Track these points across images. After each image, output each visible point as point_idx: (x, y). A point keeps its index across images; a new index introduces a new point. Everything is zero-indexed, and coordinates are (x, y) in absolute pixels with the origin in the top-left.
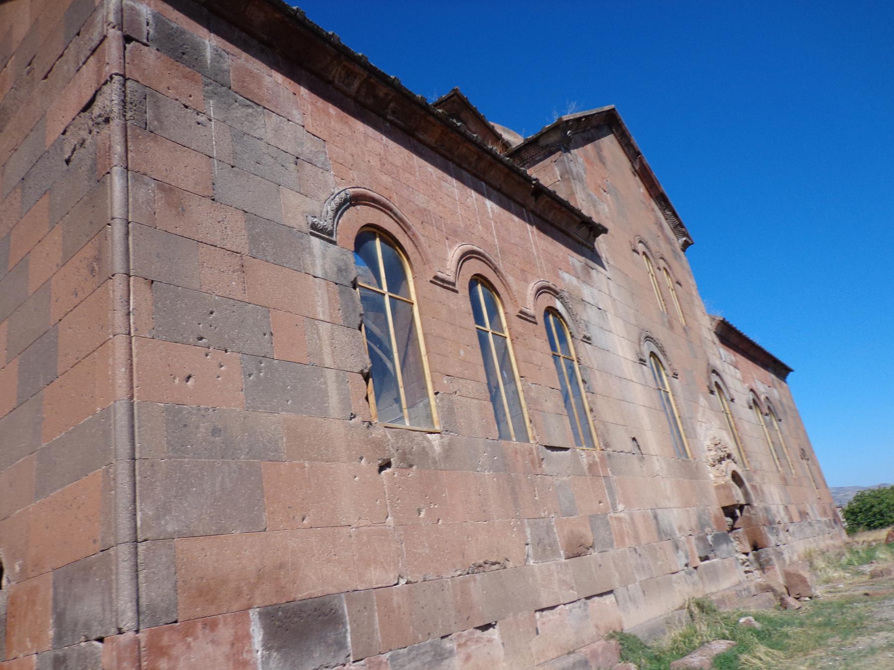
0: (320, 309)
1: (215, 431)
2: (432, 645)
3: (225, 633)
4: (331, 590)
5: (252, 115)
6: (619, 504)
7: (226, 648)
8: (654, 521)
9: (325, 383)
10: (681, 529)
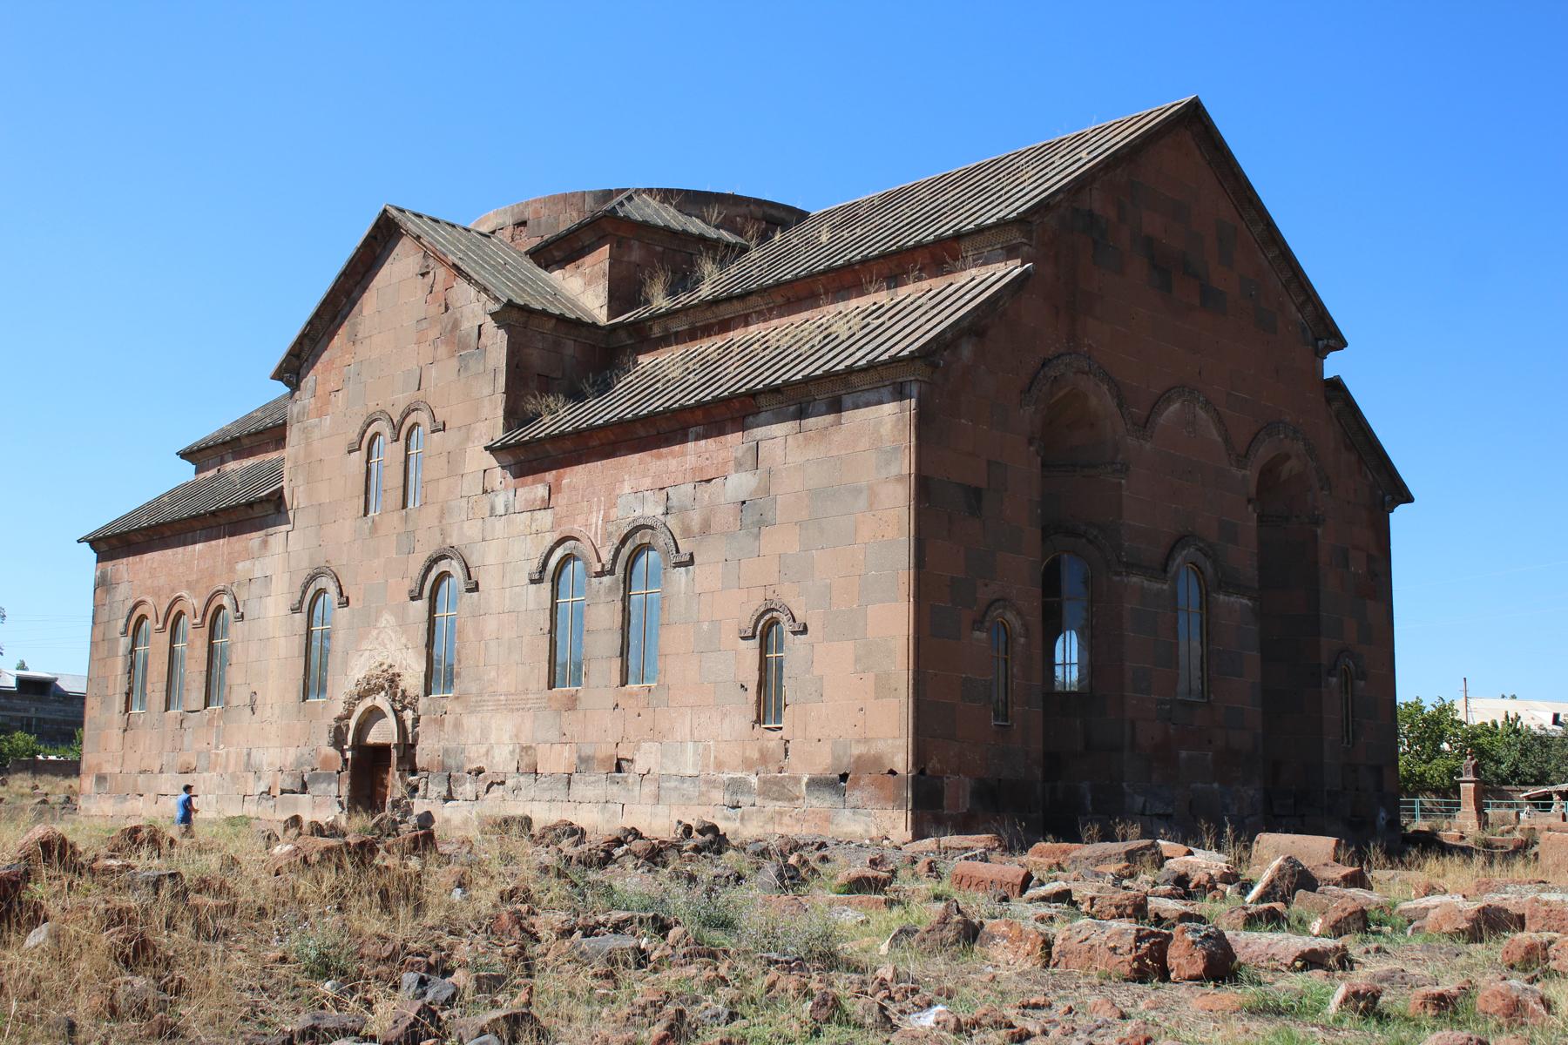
8: (246, 758)
10: (271, 764)
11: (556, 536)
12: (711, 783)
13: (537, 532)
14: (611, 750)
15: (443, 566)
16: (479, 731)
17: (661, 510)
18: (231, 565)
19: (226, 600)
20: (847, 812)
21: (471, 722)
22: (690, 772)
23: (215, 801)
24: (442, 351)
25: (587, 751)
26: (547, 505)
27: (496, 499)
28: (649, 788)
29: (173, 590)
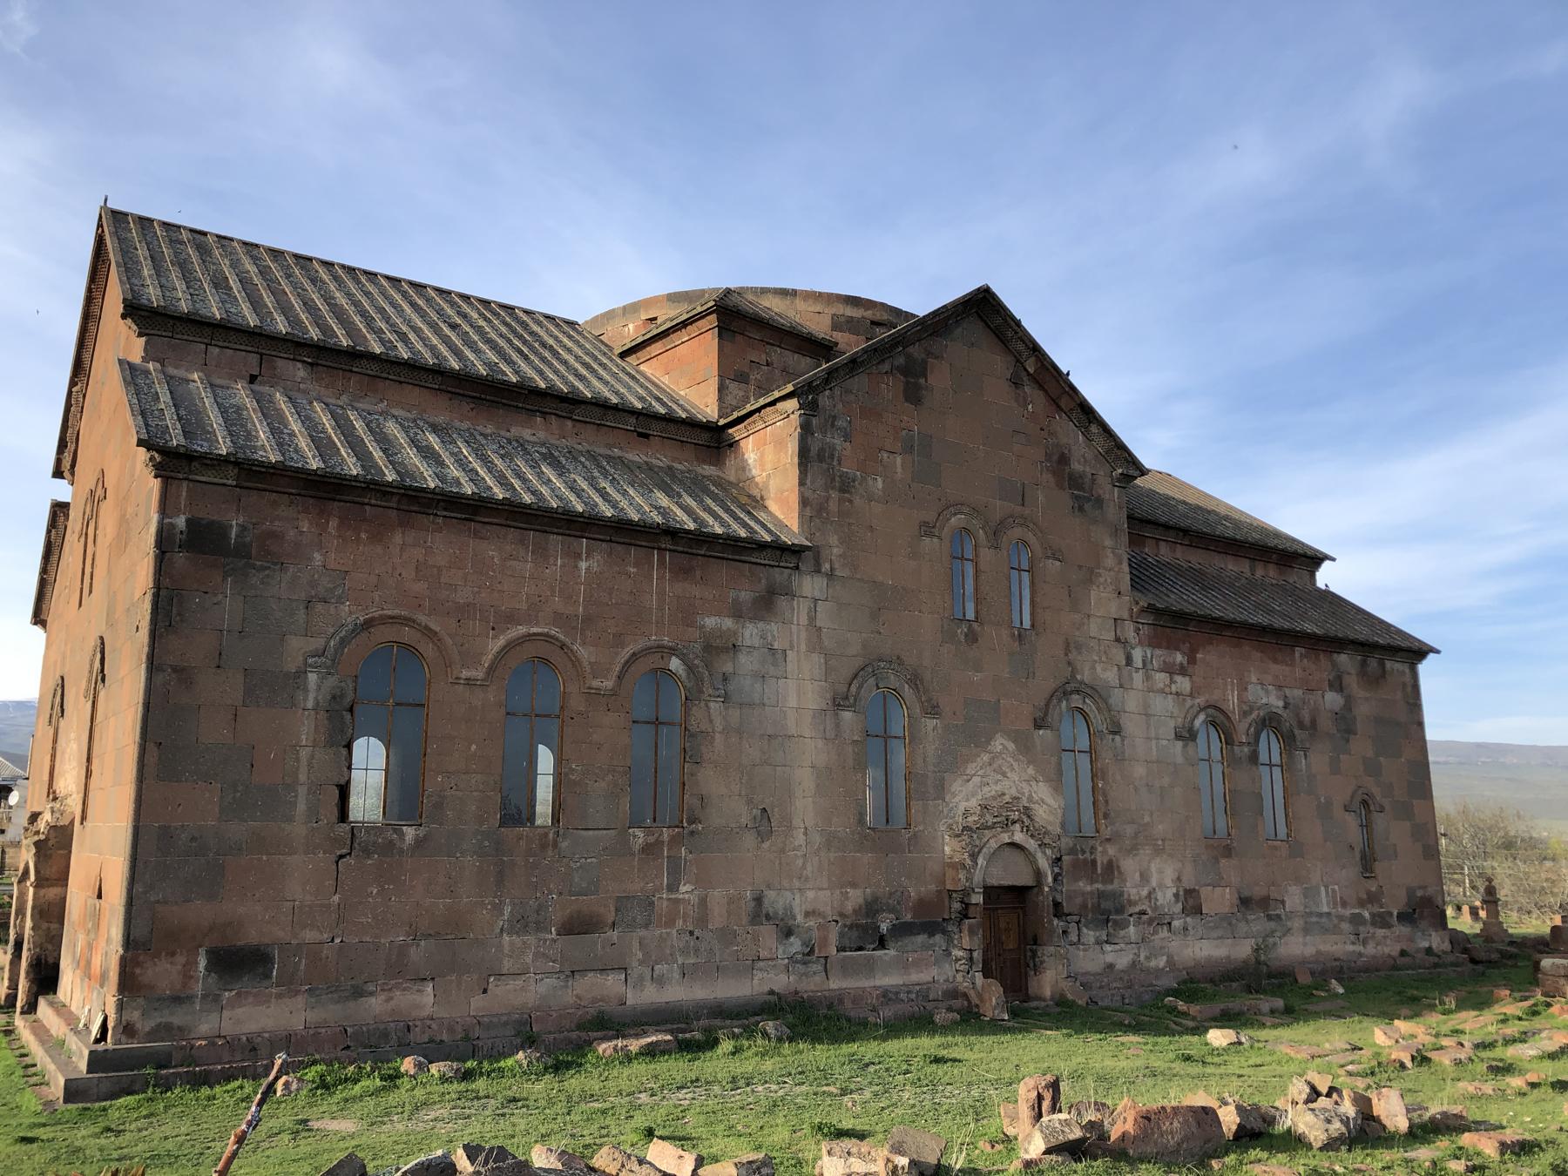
0: (304, 737)
1: (193, 839)
2: (352, 986)
3: (181, 959)
4: (266, 941)
5: (268, 576)
6: (685, 885)
7: (180, 967)
8: (753, 904)
9: (296, 796)
11: (1201, 700)
12: (1341, 918)
13: (1177, 694)
14: (1264, 892)
15: (1076, 700)
16: (1138, 874)
17: (1281, 704)
18: (687, 614)
19: (675, 664)
20: (1420, 934)
21: (1129, 865)
22: (1325, 909)
23: (676, 975)
24: (1048, 478)
25: (1246, 893)
26: (1183, 671)
27: (1133, 652)
28: (1297, 924)
29: (511, 618)
